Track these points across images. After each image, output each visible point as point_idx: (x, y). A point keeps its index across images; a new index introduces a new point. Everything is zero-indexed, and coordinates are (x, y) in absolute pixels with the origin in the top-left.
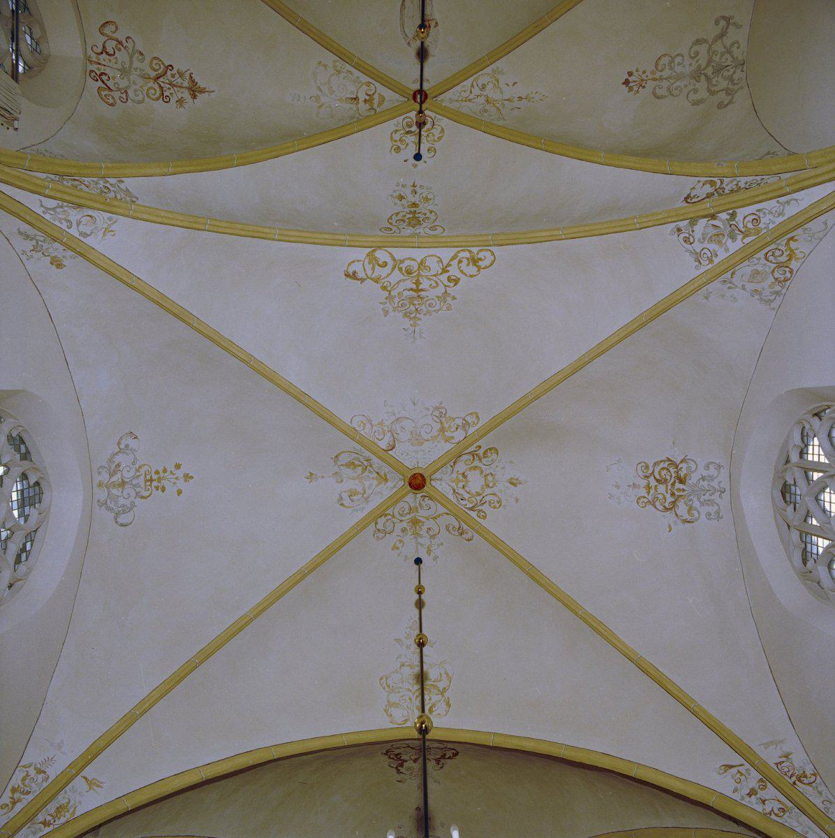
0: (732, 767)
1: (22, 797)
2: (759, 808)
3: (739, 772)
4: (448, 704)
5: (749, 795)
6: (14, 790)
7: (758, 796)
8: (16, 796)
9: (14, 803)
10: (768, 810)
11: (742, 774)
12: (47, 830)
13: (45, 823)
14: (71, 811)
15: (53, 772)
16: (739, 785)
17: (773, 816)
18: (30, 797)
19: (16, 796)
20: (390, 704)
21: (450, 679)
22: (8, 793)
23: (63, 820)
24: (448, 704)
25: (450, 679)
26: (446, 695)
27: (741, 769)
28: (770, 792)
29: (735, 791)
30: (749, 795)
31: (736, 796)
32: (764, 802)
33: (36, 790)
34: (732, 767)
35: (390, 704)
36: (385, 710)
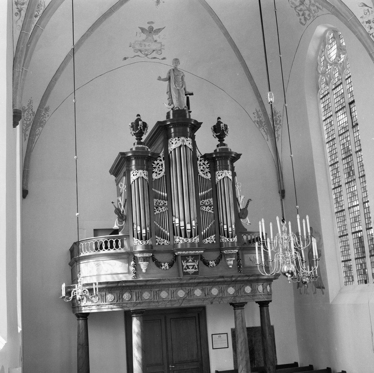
0: (366, 6)
1: (22, 6)
2: (368, 30)
3: (368, 10)
5: (367, 22)
7: (370, 25)
8: (19, 6)
9: (20, 11)
10: (370, 33)
11: (369, 12)
12: (38, 19)
13: (36, 16)
14: (43, 5)
16: (365, 16)
17: (371, 36)
18: (25, 6)
19: (19, 6)
22: (15, 6)
23: (42, 11)
27: (370, 9)
29: (362, 17)
30: (367, 22)
31: (361, 20)
32: (371, 28)
34: (366, 6)
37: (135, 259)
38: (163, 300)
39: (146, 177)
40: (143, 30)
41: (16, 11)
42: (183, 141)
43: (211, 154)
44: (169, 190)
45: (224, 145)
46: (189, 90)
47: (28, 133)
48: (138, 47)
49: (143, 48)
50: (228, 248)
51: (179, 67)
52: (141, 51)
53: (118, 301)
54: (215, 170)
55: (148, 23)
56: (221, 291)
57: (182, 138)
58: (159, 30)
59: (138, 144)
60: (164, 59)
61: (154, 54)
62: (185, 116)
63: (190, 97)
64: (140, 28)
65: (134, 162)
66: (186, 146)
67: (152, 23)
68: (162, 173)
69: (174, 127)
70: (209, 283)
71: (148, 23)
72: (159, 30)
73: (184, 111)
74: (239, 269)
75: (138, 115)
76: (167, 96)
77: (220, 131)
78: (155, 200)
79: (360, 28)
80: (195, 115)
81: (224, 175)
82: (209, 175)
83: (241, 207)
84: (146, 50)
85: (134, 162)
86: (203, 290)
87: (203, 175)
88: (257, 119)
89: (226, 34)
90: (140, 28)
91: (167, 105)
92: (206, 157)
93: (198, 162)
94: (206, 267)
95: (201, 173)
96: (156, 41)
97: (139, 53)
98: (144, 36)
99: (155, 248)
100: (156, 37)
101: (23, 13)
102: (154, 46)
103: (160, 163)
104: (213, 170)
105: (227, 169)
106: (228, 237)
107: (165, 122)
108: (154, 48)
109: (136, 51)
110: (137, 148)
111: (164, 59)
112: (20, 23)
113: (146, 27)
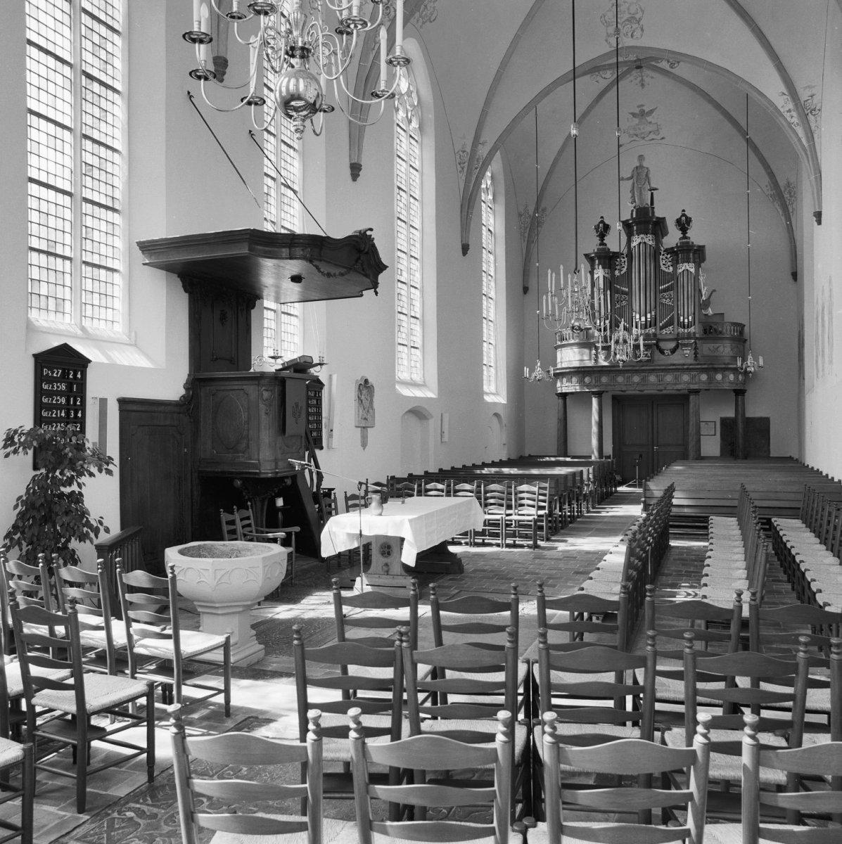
2: (789, 119)
4: (642, 30)
5: (788, 112)
6: (460, 164)
13: (476, 168)
15: (468, 149)
19: (462, 165)
20: (608, 35)
21: (643, 11)
24: (642, 30)
25: (643, 11)
26: (641, 23)
28: (794, 114)
30: (788, 112)
31: (782, 110)
33: (467, 159)
35: (608, 35)
36: (606, 41)
37: (596, 348)
38: (619, 384)
39: (607, 275)
40: (634, 115)
41: (459, 169)
42: (642, 238)
43: (672, 248)
44: (630, 287)
45: (686, 238)
46: (653, 185)
47: (526, 235)
48: (632, 132)
49: (638, 132)
50: (684, 339)
51: (645, 164)
52: (637, 135)
53: (581, 382)
54: (678, 263)
55: (638, 107)
56: (676, 378)
57: (642, 236)
58: (651, 112)
59: (600, 245)
60: (663, 138)
61: (652, 136)
62: (648, 213)
63: (655, 192)
64: (632, 113)
65: (597, 261)
66: (645, 243)
67: (643, 106)
68: (624, 270)
69: (637, 225)
70: (662, 370)
71: (638, 107)
72: (651, 112)
73: (648, 208)
74: (696, 357)
75: (602, 217)
76: (630, 195)
77: (684, 224)
78: (617, 295)
79: (781, 119)
80: (659, 213)
81: (683, 268)
82: (671, 268)
83: (704, 298)
84: (642, 133)
85: (597, 261)
86: (657, 376)
87: (664, 269)
88: (770, 192)
89: (718, 106)
90: (632, 113)
91: (630, 205)
92: (670, 251)
93: (661, 257)
94: (662, 356)
95: (663, 268)
96: (650, 123)
97: (635, 138)
98: (636, 121)
99: (659, 337)
100: (649, 119)
101: (465, 170)
102: (649, 128)
103: (623, 260)
104: (675, 263)
105: (689, 262)
106: (684, 328)
107: (628, 220)
108: (651, 129)
109: (630, 136)
110: (598, 249)
111: (663, 138)
112: (464, 178)
113: (637, 111)
